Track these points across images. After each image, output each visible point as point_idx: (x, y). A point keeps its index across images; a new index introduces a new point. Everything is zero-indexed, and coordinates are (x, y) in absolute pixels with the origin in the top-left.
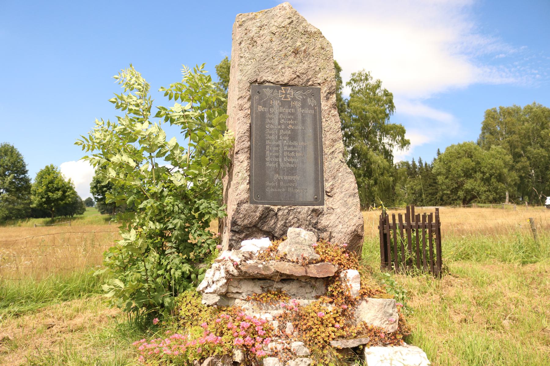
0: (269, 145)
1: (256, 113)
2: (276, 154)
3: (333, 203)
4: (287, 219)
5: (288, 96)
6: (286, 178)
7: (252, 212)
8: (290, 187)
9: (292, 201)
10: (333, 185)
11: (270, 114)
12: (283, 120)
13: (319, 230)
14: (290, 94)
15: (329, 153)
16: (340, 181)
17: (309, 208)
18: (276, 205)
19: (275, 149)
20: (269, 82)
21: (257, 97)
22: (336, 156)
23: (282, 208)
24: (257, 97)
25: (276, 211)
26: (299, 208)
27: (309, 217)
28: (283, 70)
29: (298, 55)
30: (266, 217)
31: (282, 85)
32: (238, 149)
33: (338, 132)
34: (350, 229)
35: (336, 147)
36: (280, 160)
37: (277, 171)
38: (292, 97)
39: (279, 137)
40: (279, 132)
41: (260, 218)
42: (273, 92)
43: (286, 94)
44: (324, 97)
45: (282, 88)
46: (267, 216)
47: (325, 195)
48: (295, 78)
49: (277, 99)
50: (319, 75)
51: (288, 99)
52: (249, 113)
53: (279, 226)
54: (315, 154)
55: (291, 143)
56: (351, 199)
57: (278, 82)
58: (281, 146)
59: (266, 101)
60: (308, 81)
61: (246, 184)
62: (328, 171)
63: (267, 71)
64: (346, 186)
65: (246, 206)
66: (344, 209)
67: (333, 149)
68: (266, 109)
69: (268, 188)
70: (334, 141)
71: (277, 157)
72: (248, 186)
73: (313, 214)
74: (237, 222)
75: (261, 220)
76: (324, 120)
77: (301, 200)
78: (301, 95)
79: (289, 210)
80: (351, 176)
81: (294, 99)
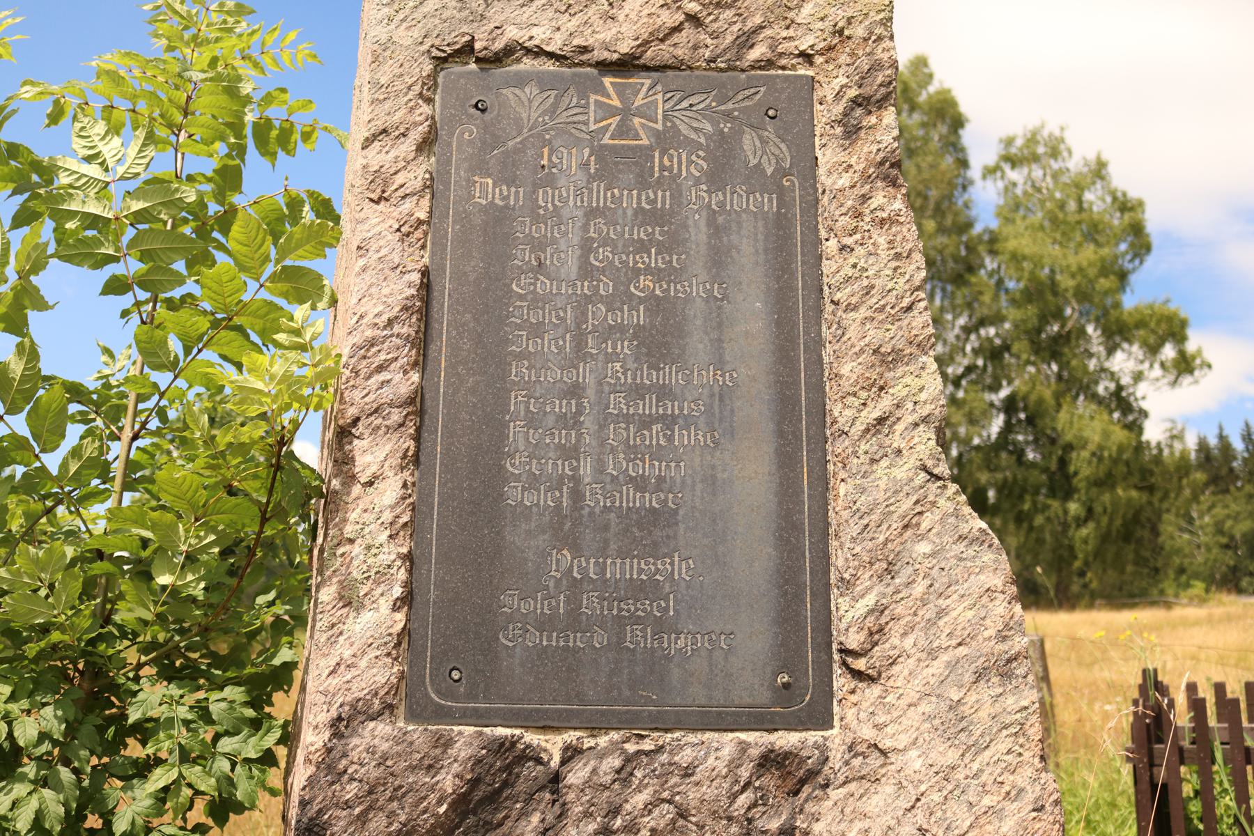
0: (528, 386)
2: (561, 437)
3: (881, 719)
4: (615, 811)
5: (637, 120)
7: (412, 768)
8: (638, 620)
10: (879, 610)
11: (537, 219)
12: (605, 252)
14: (646, 113)
15: (859, 427)
16: (919, 589)
17: (743, 747)
18: (557, 729)
19: (561, 406)
20: (538, 52)
21: (469, 131)
23: (588, 743)
24: (469, 131)
25: (555, 762)
27: (744, 799)
30: (493, 798)
31: (605, 67)
33: (909, 308)
35: (898, 391)
36: (586, 469)
38: (659, 126)
39: (580, 344)
40: (581, 318)
41: (462, 804)
43: (626, 112)
44: (832, 124)
45: (608, 81)
46: (499, 791)
47: (837, 670)
48: (677, 29)
49: (577, 142)
52: (422, 215)
54: (780, 434)
55: (648, 377)
56: (985, 692)
57: (585, 50)
58: (591, 392)
59: (516, 150)
60: (746, 40)
61: (385, 605)
62: (855, 531)
64: (961, 613)
65: (378, 734)
67: (885, 404)
68: (516, 196)
69: (514, 630)
70: (889, 359)
71: (571, 453)
72: (400, 617)
73: (769, 781)
74: (328, 824)
75: (464, 816)
76: (832, 245)
77: (697, 695)
78: (708, 113)
79: (629, 759)
80: (988, 557)
81: (667, 140)
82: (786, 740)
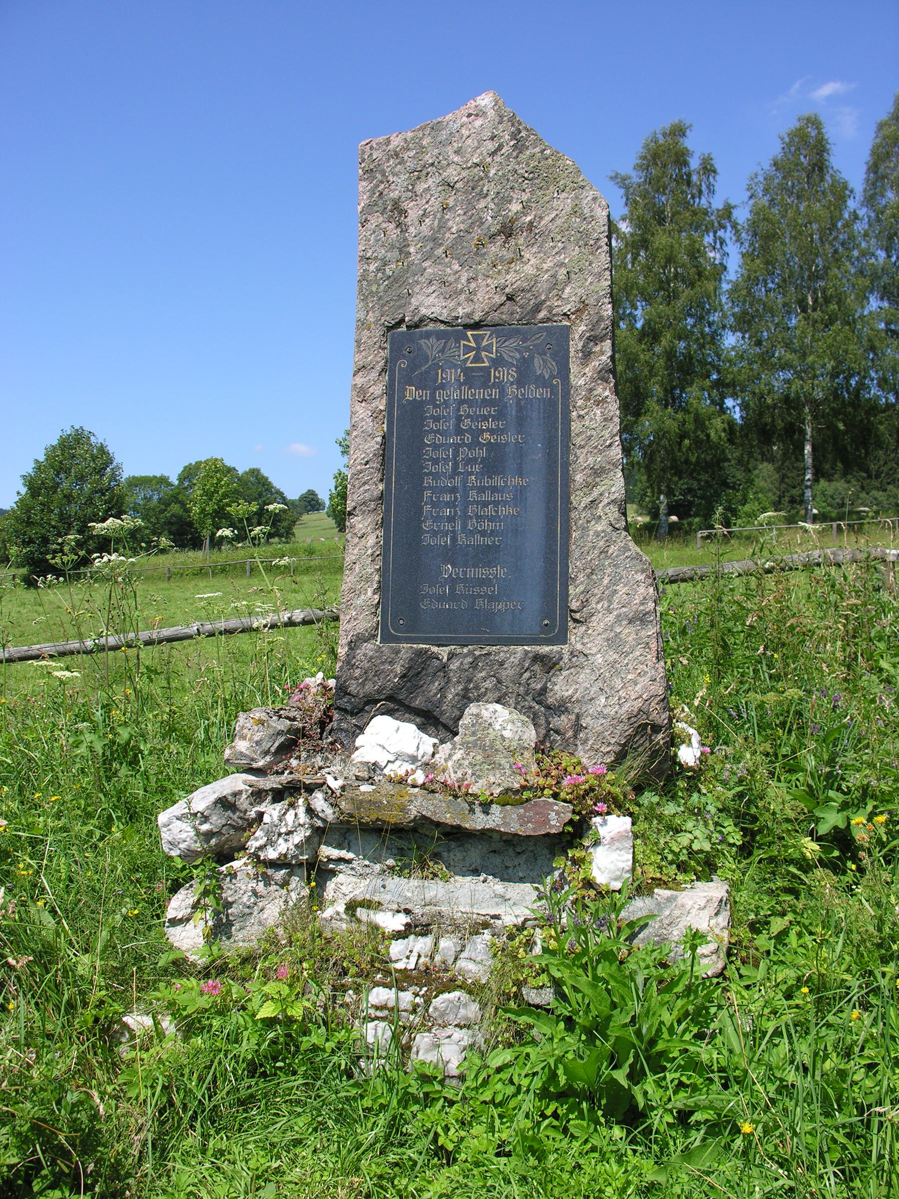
1: (401, 407)
4: (470, 681)
5: (483, 354)
6: (471, 573)
7: (383, 663)
8: (481, 596)
9: (486, 633)
12: (468, 421)
13: (548, 707)
14: (488, 348)
15: (583, 505)
17: (526, 653)
20: (436, 320)
22: (599, 512)
23: (459, 651)
26: (501, 652)
27: (527, 675)
28: (473, 285)
29: (513, 242)
31: (467, 327)
32: (353, 504)
33: (610, 445)
34: (626, 707)
36: (458, 527)
37: (451, 554)
38: (494, 356)
42: (444, 347)
43: (478, 349)
45: (469, 333)
46: (419, 673)
49: (455, 366)
50: (568, 290)
51: (483, 362)
53: (450, 696)
54: (548, 508)
59: (426, 372)
60: (537, 308)
61: (370, 592)
63: (431, 289)
65: (368, 648)
66: (613, 656)
67: (595, 493)
69: (426, 601)
70: (598, 472)
72: (377, 597)
73: (537, 668)
74: (349, 686)
79: (476, 658)
81: (498, 362)
82: (545, 649)
